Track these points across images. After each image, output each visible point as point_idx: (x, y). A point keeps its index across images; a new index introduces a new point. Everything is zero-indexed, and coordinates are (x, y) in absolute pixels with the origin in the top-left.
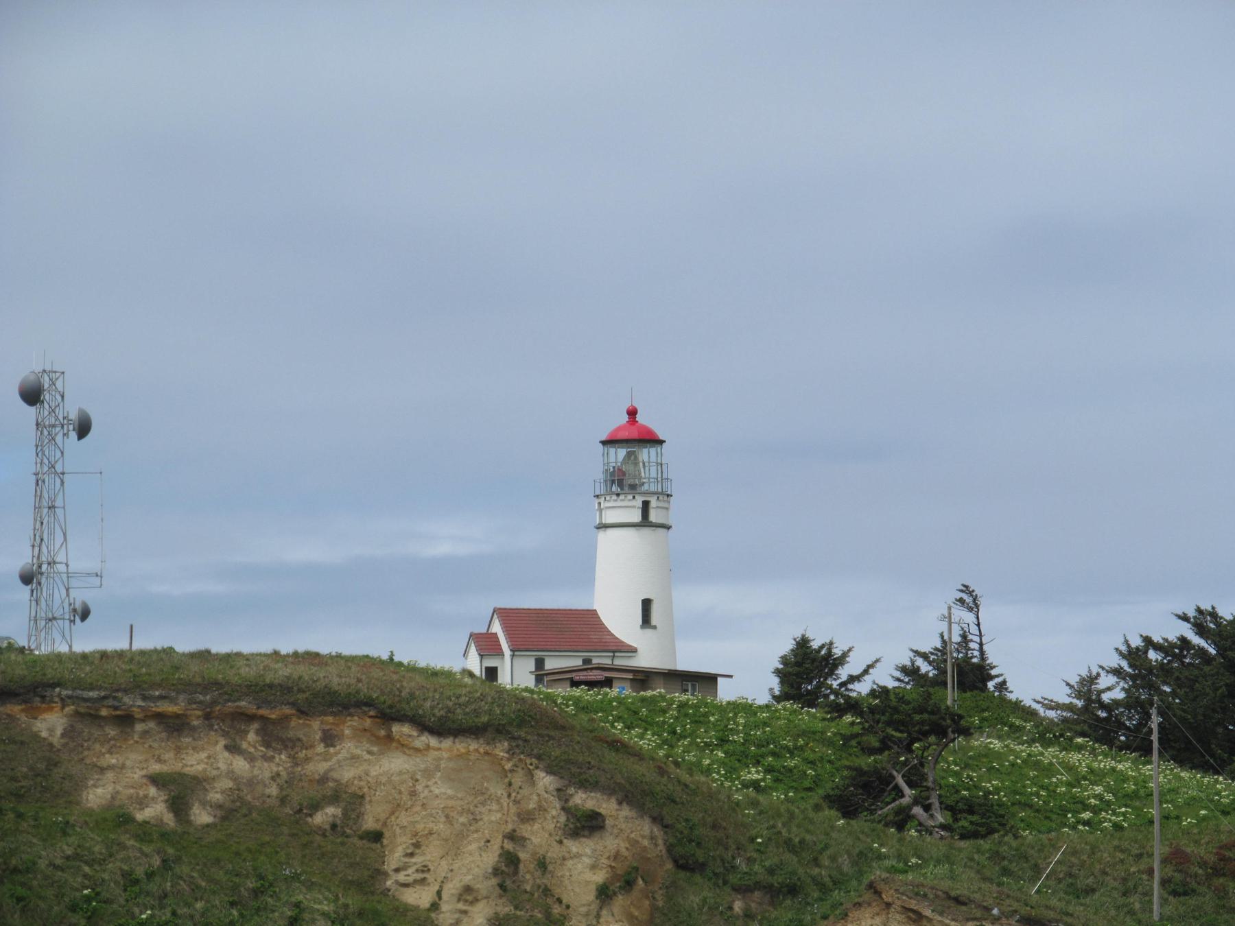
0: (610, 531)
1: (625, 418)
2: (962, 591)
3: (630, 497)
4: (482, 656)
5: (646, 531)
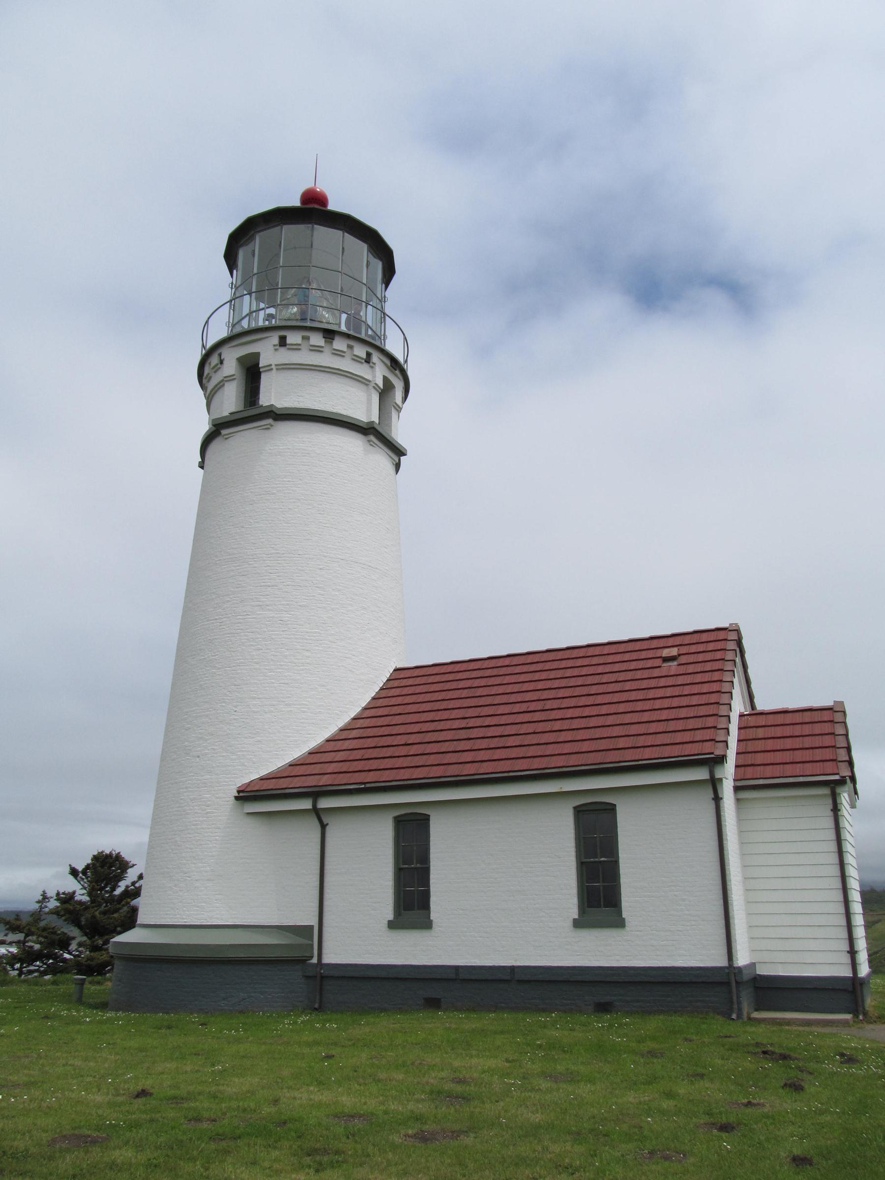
3: (361, 351)
5: (381, 459)
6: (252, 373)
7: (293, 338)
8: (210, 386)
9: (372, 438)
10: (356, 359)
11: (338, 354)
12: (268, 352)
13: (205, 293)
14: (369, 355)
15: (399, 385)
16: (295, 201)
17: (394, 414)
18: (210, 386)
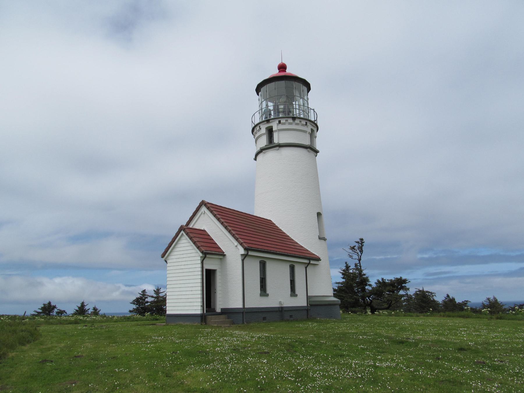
2: (358, 242)
3: (304, 122)
4: (205, 255)
6: (270, 131)
7: (283, 121)
9: (309, 150)
10: (303, 125)
11: (297, 124)
12: (275, 125)
13: (253, 106)
14: (306, 123)
15: (315, 129)
18: (257, 136)
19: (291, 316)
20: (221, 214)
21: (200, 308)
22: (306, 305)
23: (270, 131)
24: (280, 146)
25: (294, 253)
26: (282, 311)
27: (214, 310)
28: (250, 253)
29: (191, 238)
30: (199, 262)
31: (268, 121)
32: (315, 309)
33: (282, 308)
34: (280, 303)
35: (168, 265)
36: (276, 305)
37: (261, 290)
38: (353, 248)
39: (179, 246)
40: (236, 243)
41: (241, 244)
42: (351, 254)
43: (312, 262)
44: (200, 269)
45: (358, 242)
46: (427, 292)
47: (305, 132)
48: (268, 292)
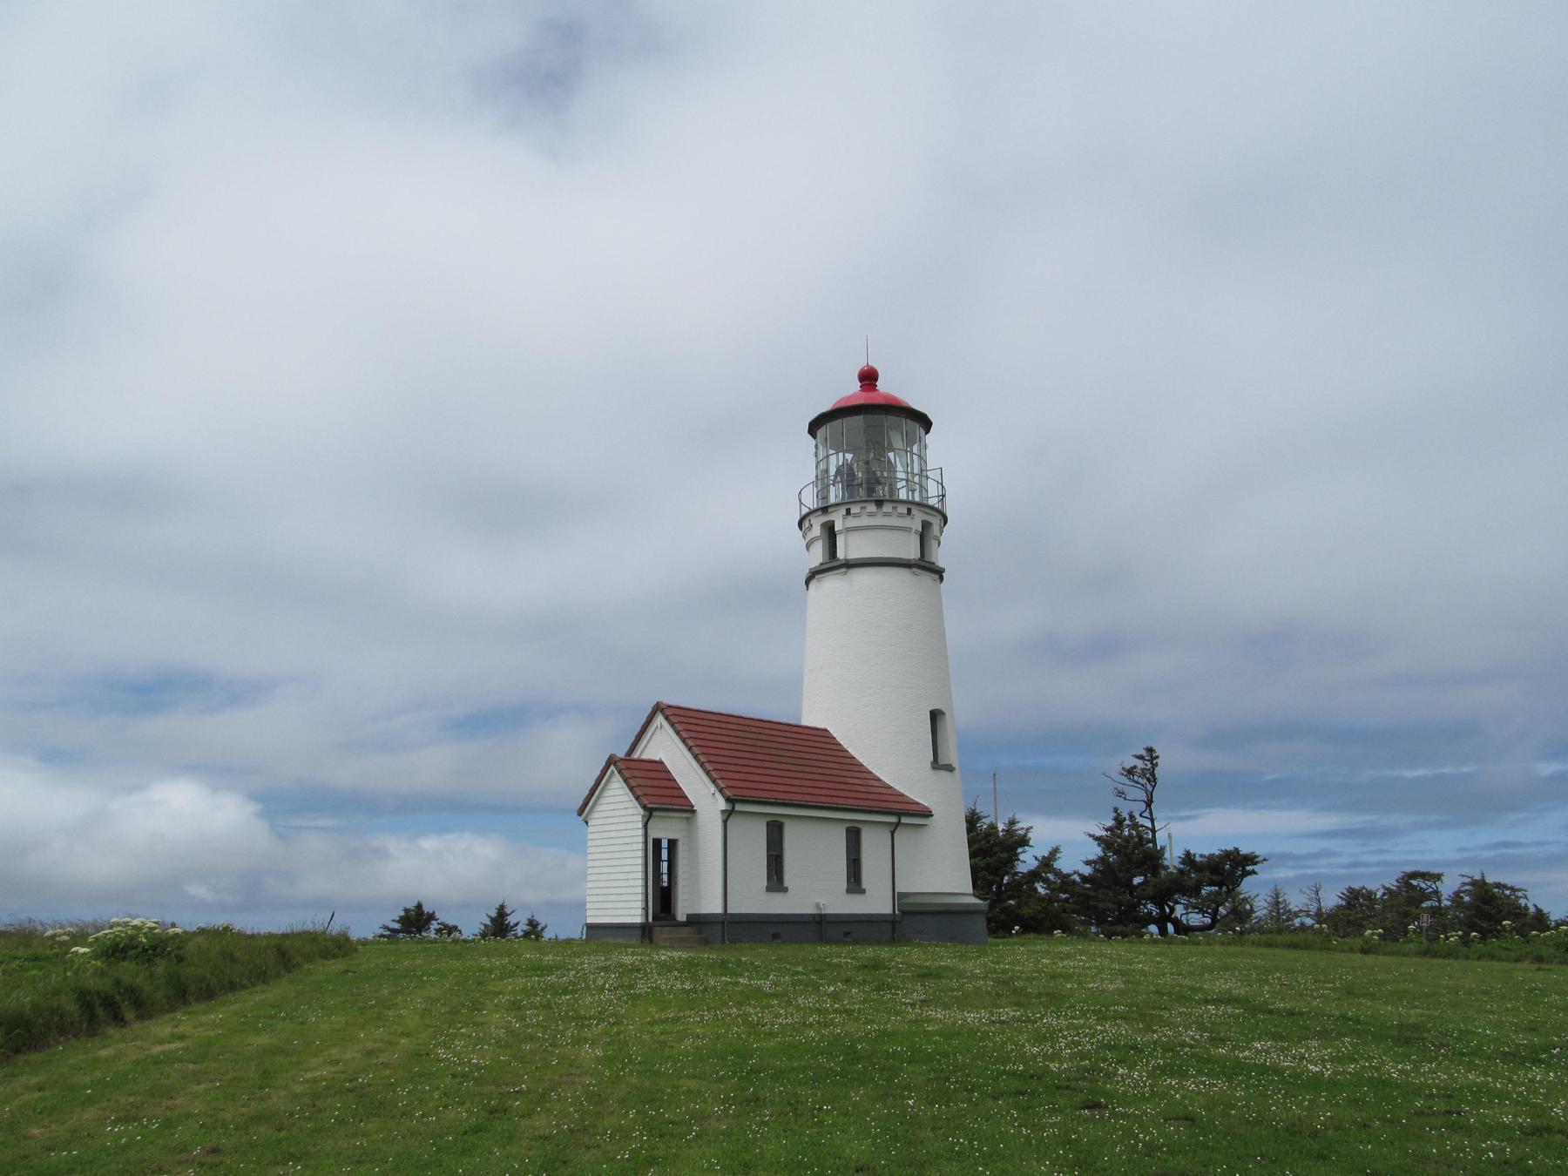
0: (862, 577)
1: (855, 386)
2: (1141, 757)
4: (649, 813)
5: (927, 578)
6: (830, 532)
7: (855, 509)
8: (809, 537)
10: (901, 515)
11: (887, 515)
15: (936, 521)
16: (850, 388)
17: (934, 543)
19: (847, 934)
20: (695, 727)
21: (640, 912)
22: (889, 910)
23: (830, 530)
24: (850, 565)
25: (857, 802)
26: (820, 923)
27: (674, 918)
28: (738, 807)
29: (626, 780)
30: (640, 825)
31: (825, 510)
32: (915, 920)
33: (822, 916)
34: (817, 905)
35: (590, 829)
36: (808, 909)
37: (769, 878)
38: (1130, 772)
39: (607, 793)
40: (713, 789)
41: (721, 791)
42: (1120, 787)
43: (904, 820)
44: (641, 839)
45: (1141, 757)
46: (1498, 885)
47: (907, 530)
48: (787, 882)
